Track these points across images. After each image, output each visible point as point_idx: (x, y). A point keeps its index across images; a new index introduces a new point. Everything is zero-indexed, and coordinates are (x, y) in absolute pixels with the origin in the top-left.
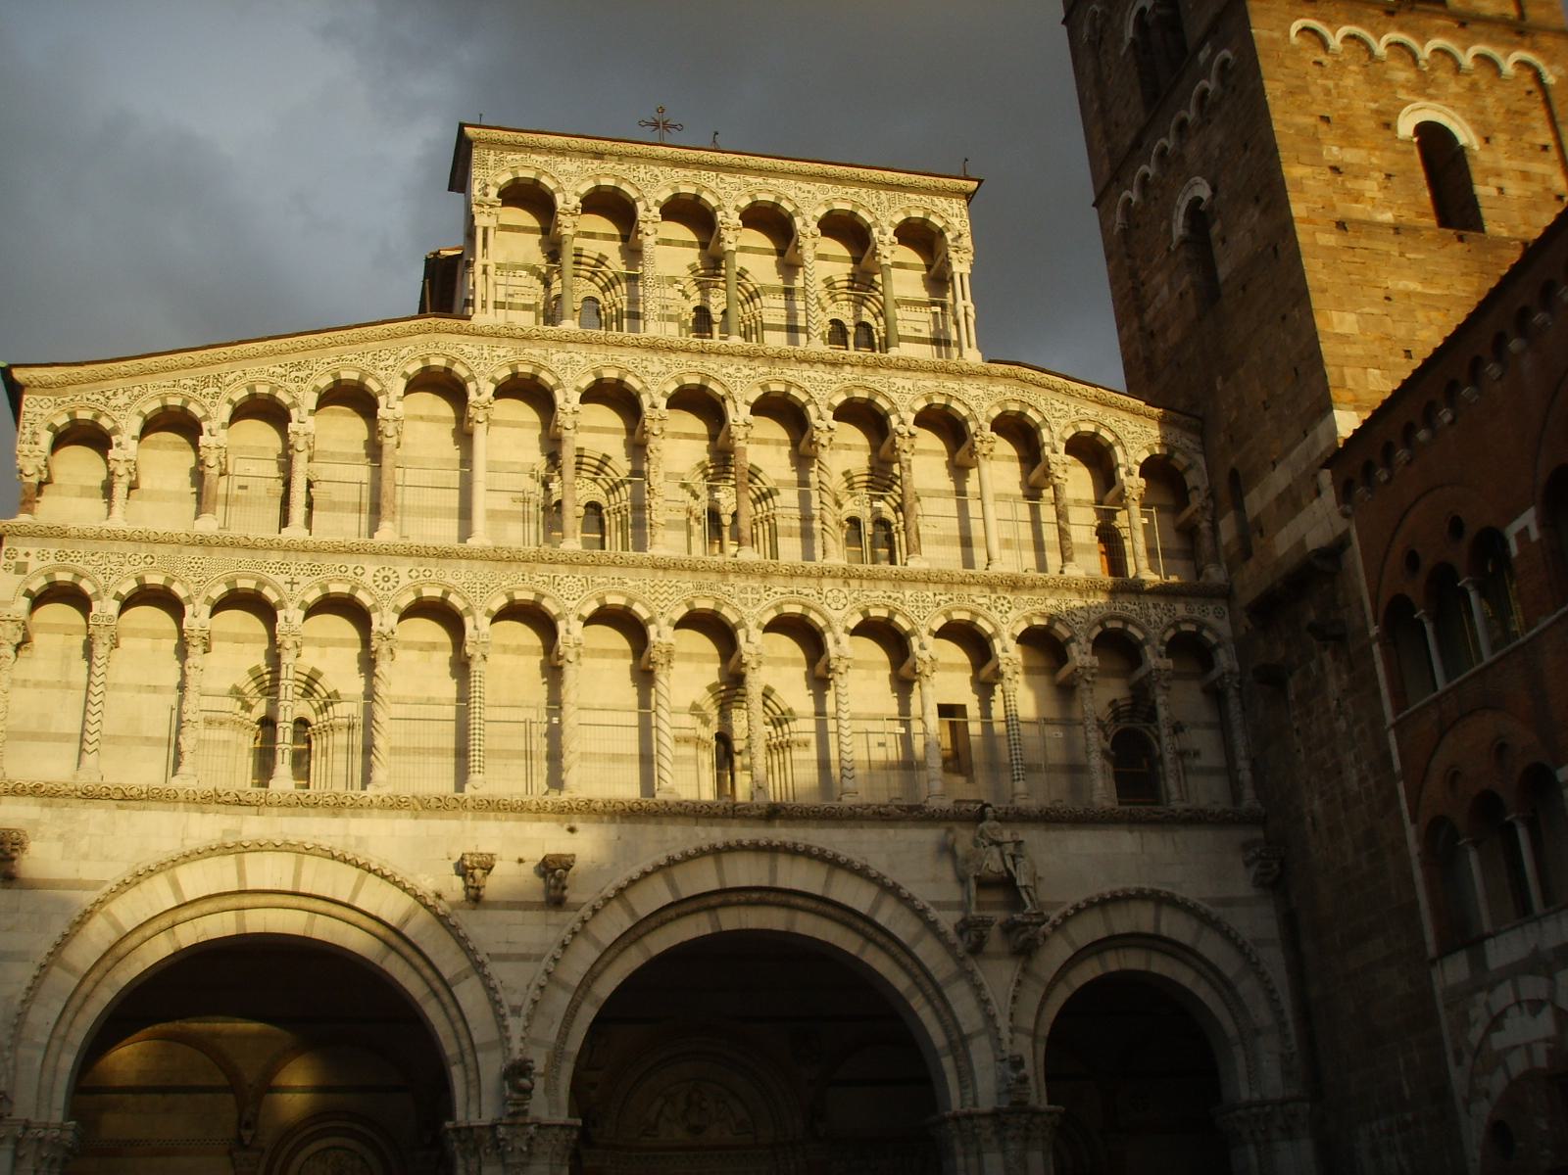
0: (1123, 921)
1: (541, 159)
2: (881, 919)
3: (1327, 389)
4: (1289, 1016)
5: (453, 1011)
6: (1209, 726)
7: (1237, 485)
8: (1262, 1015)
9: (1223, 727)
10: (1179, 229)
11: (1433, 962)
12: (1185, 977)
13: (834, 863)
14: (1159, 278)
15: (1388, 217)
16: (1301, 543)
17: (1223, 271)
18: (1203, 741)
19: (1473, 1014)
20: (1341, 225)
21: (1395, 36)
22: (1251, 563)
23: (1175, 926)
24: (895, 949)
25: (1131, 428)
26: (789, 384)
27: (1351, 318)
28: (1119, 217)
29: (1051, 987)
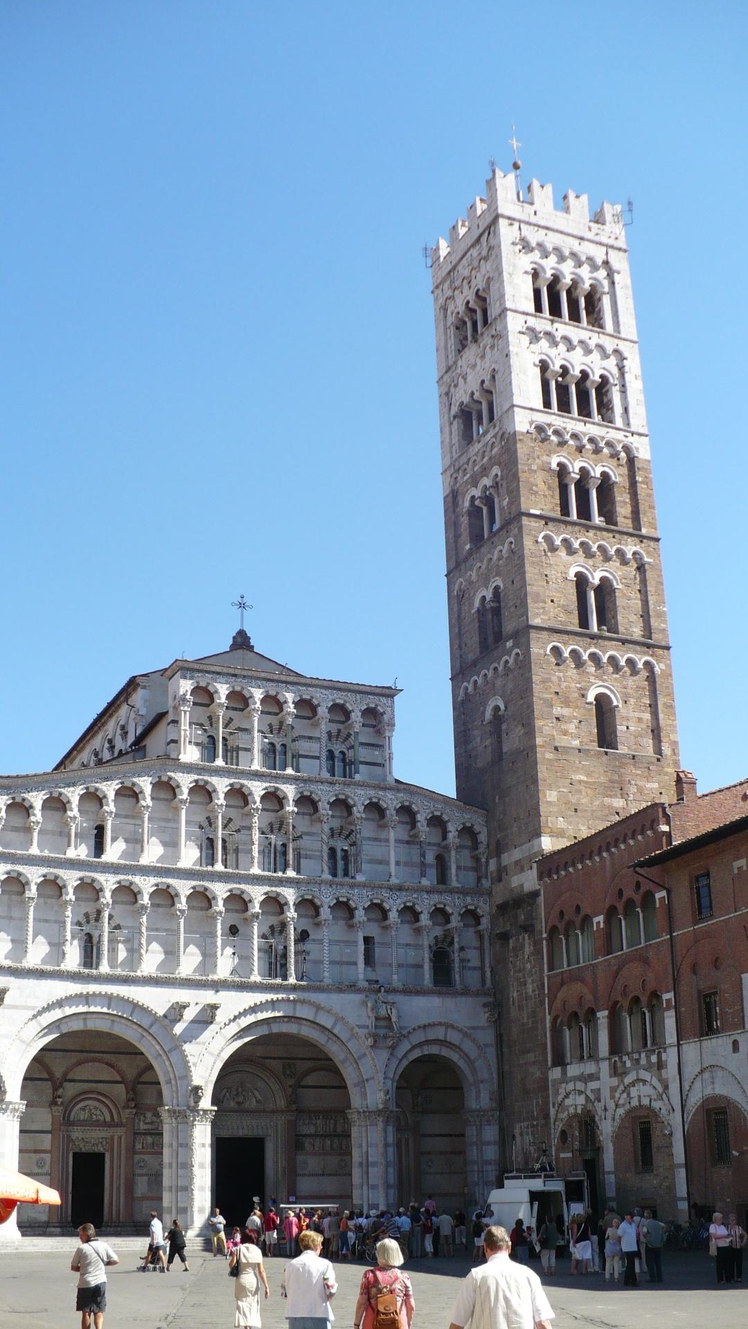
0: (433, 1034)
1: (210, 676)
2: (335, 1031)
3: (540, 826)
4: (495, 1075)
5: (167, 1063)
6: (475, 948)
7: (498, 849)
8: (486, 1076)
9: (481, 949)
10: (488, 715)
11: (549, 1069)
12: (454, 1056)
13: (318, 1008)
14: (476, 732)
15: (576, 743)
16: (522, 886)
17: (505, 750)
18: (473, 956)
19: (560, 1091)
20: (556, 749)
21: (593, 650)
22: (501, 883)
23: (454, 1037)
24: (339, 1043)
25: (457, 814)
26: (311, 793)
27: (554, 794)
28: (462, 692)
29: (401, 1060)
